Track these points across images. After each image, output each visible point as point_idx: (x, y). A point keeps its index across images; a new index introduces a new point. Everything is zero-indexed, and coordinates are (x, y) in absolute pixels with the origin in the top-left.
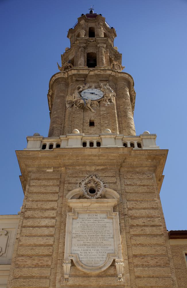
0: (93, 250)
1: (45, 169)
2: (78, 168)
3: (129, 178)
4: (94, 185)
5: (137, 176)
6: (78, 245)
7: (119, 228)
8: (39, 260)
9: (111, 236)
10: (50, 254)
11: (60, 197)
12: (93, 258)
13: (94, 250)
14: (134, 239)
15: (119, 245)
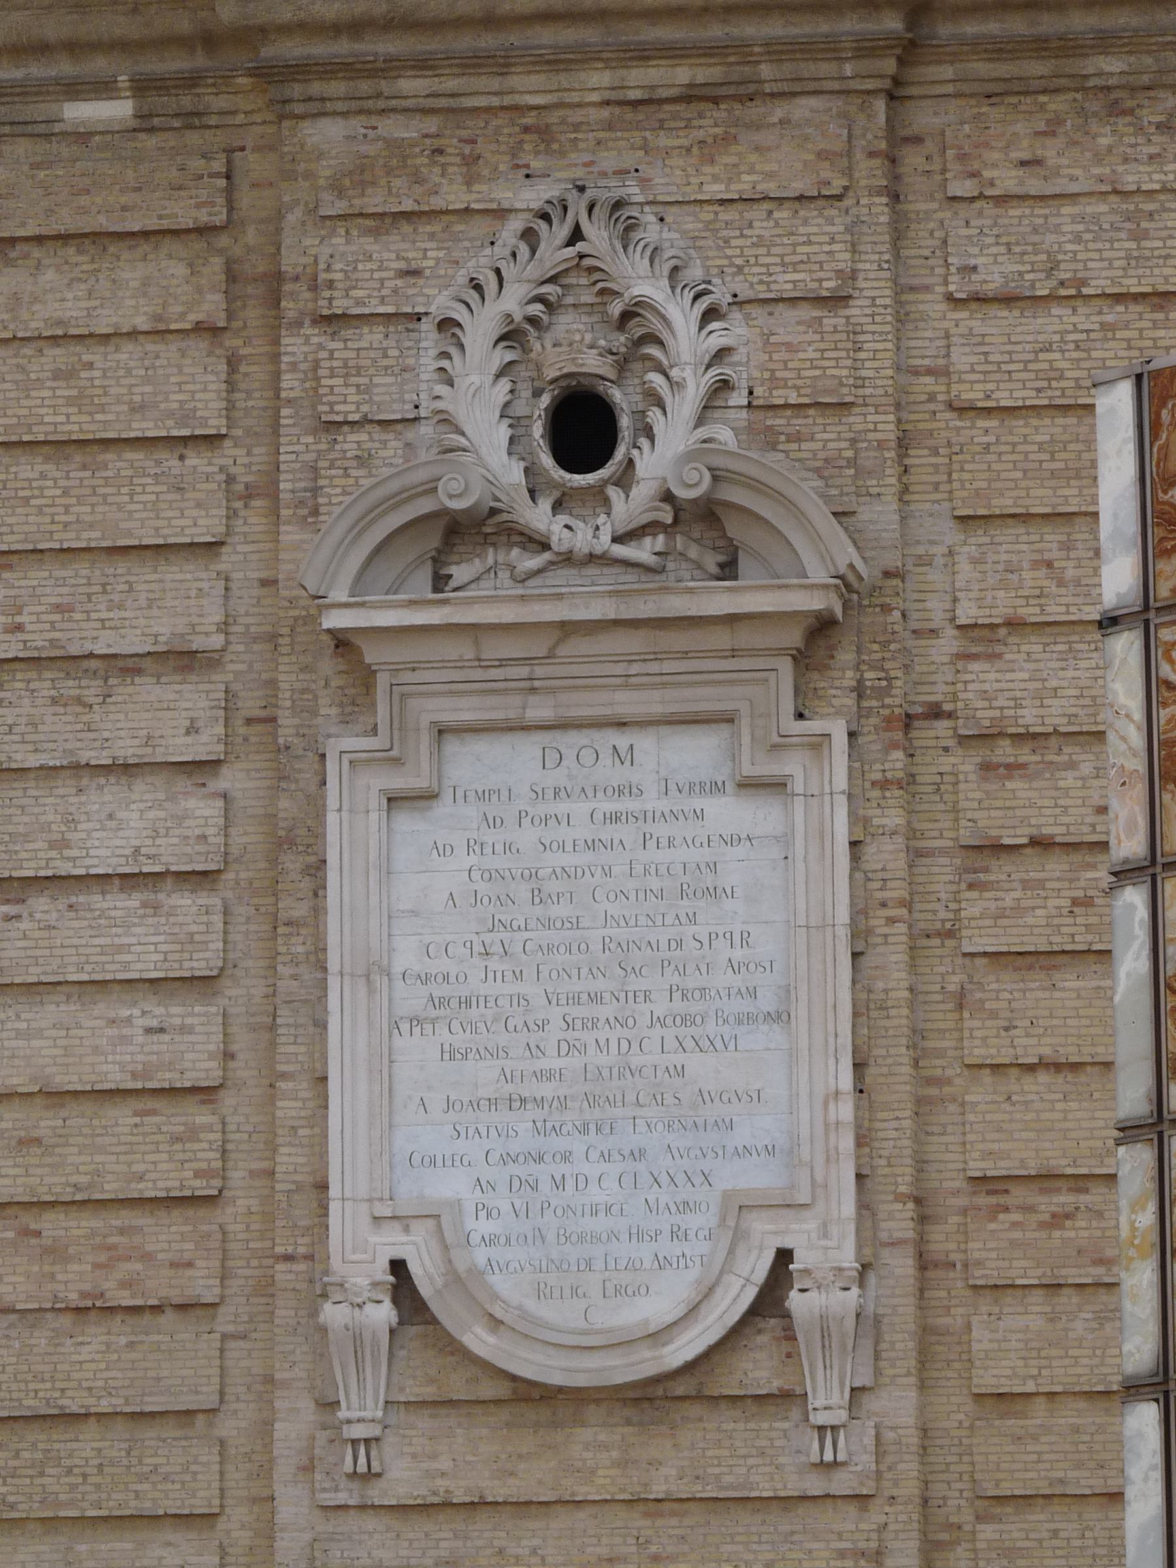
0: (594, 1155)
1: (39, 110)
2: (411, 85)
3: (1003, 200)
4: (593, 363)
5: (1098, 159)
6: (449, 1105)
7: (843, 915)
8: (102, 1258)
9: (767, 1002)
10: (202, 1187)
11: (249, 495)
12: (596, 1238)
13: (605, 1157)
14: (994, 1015)
15: (832, 1106)
